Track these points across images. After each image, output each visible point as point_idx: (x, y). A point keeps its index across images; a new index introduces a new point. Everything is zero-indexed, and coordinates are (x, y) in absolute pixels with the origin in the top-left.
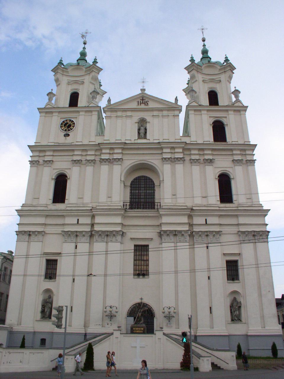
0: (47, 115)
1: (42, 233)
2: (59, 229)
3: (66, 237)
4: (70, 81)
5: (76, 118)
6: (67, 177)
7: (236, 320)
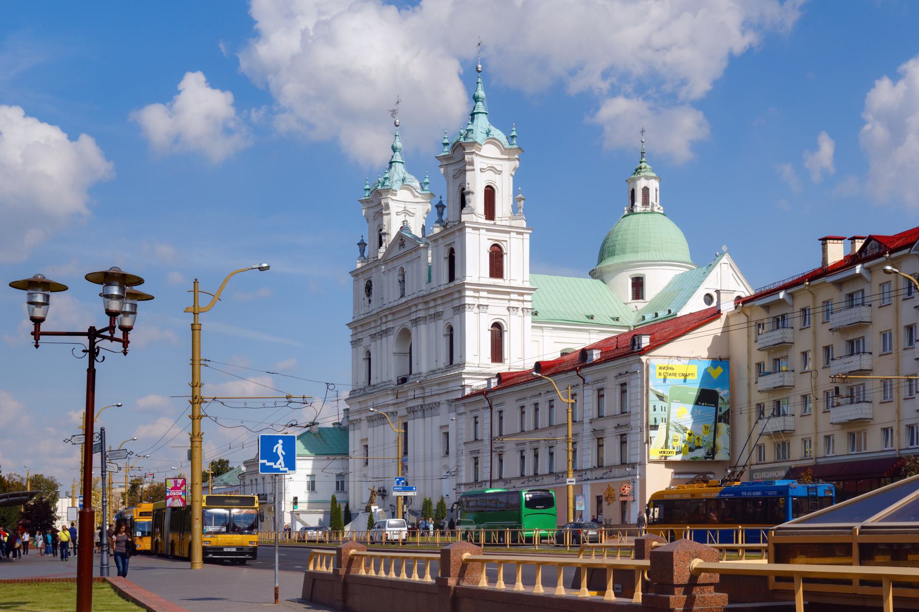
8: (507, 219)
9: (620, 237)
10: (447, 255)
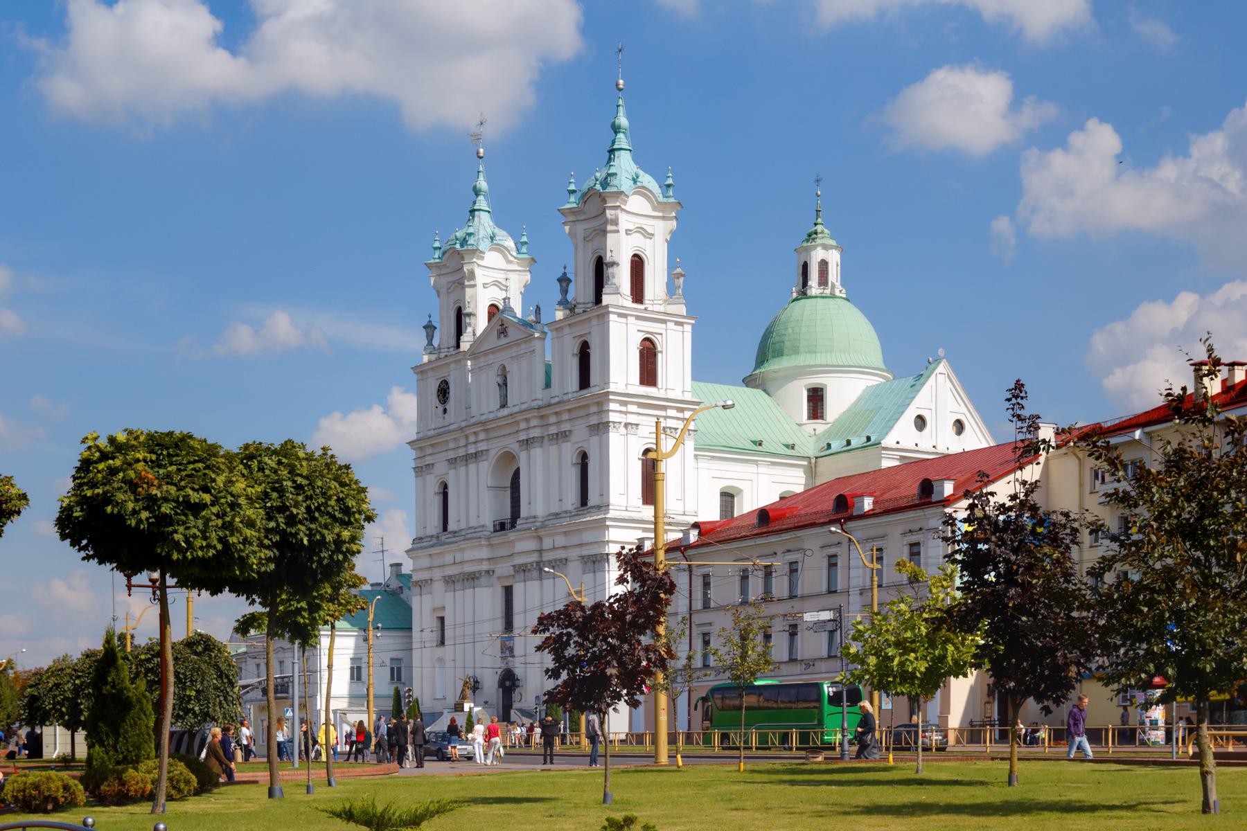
8: (661, 302)
9: (790, 330)
10: (576, 350)
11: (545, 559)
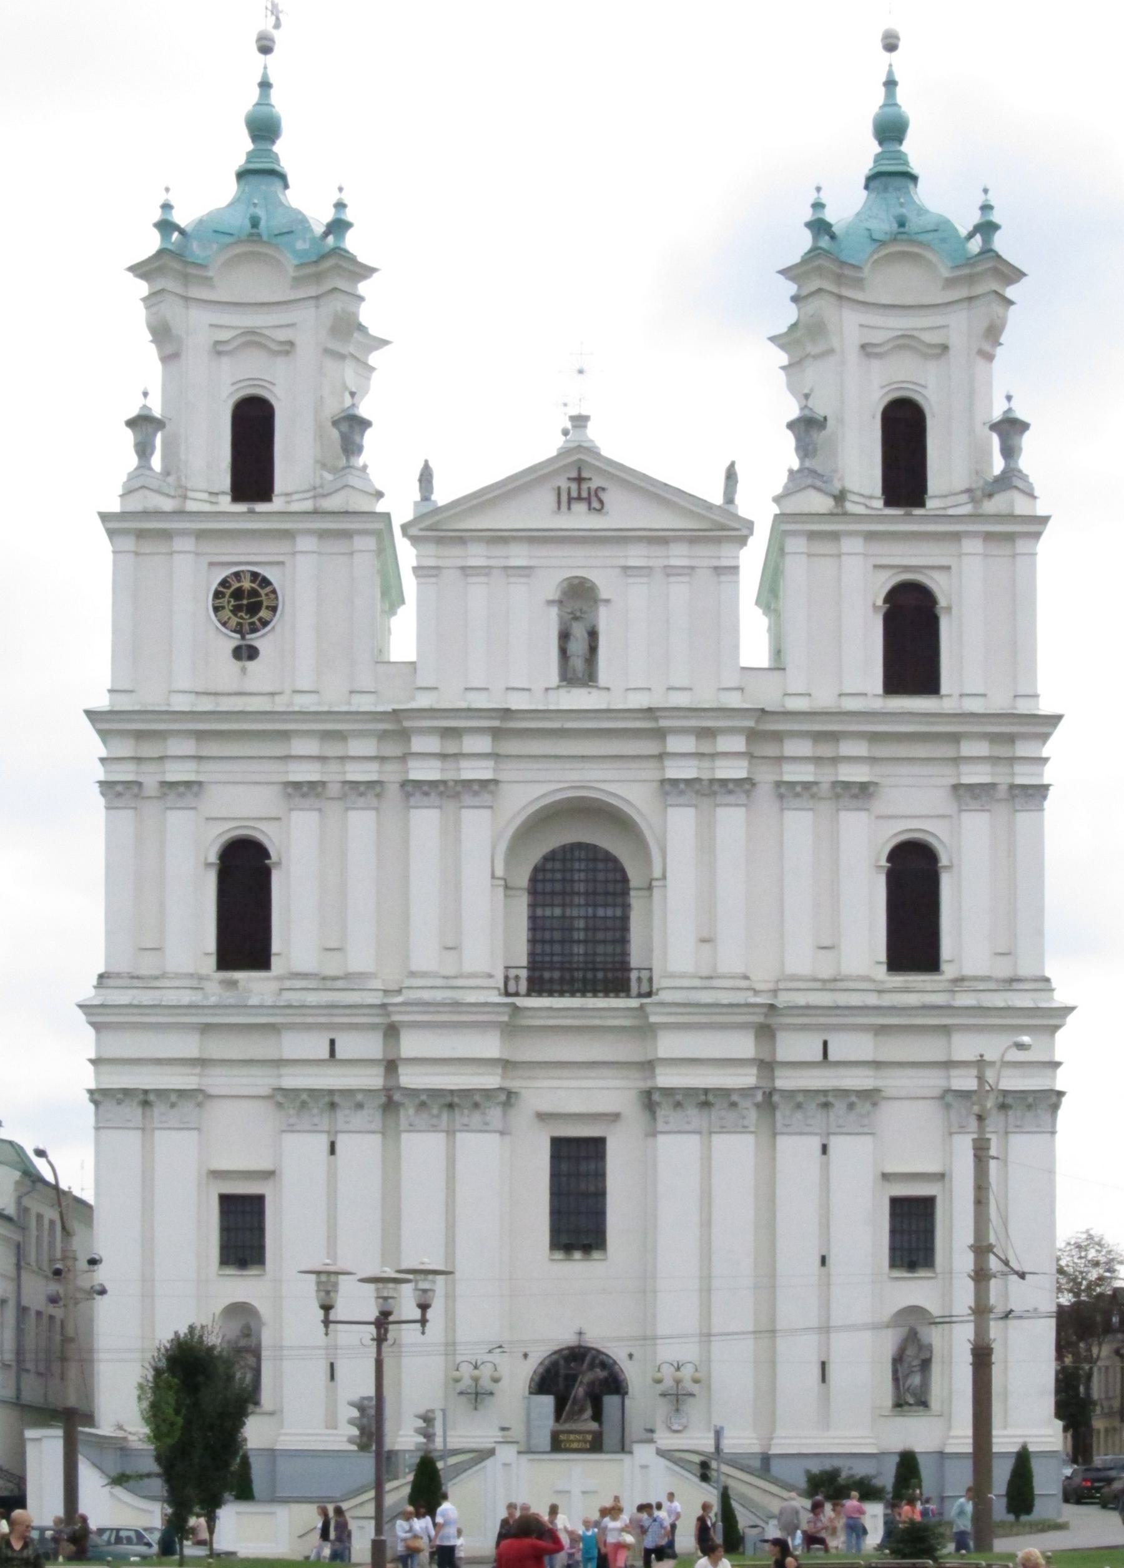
0: (147, 547)
1: (197, 1097)
2: (262, 1081)
3: (292, 1112)
4: (225, 335)
5: (282, 563)
6: (268, 856)
7: (910, 1405)
11: (780, 1084)
